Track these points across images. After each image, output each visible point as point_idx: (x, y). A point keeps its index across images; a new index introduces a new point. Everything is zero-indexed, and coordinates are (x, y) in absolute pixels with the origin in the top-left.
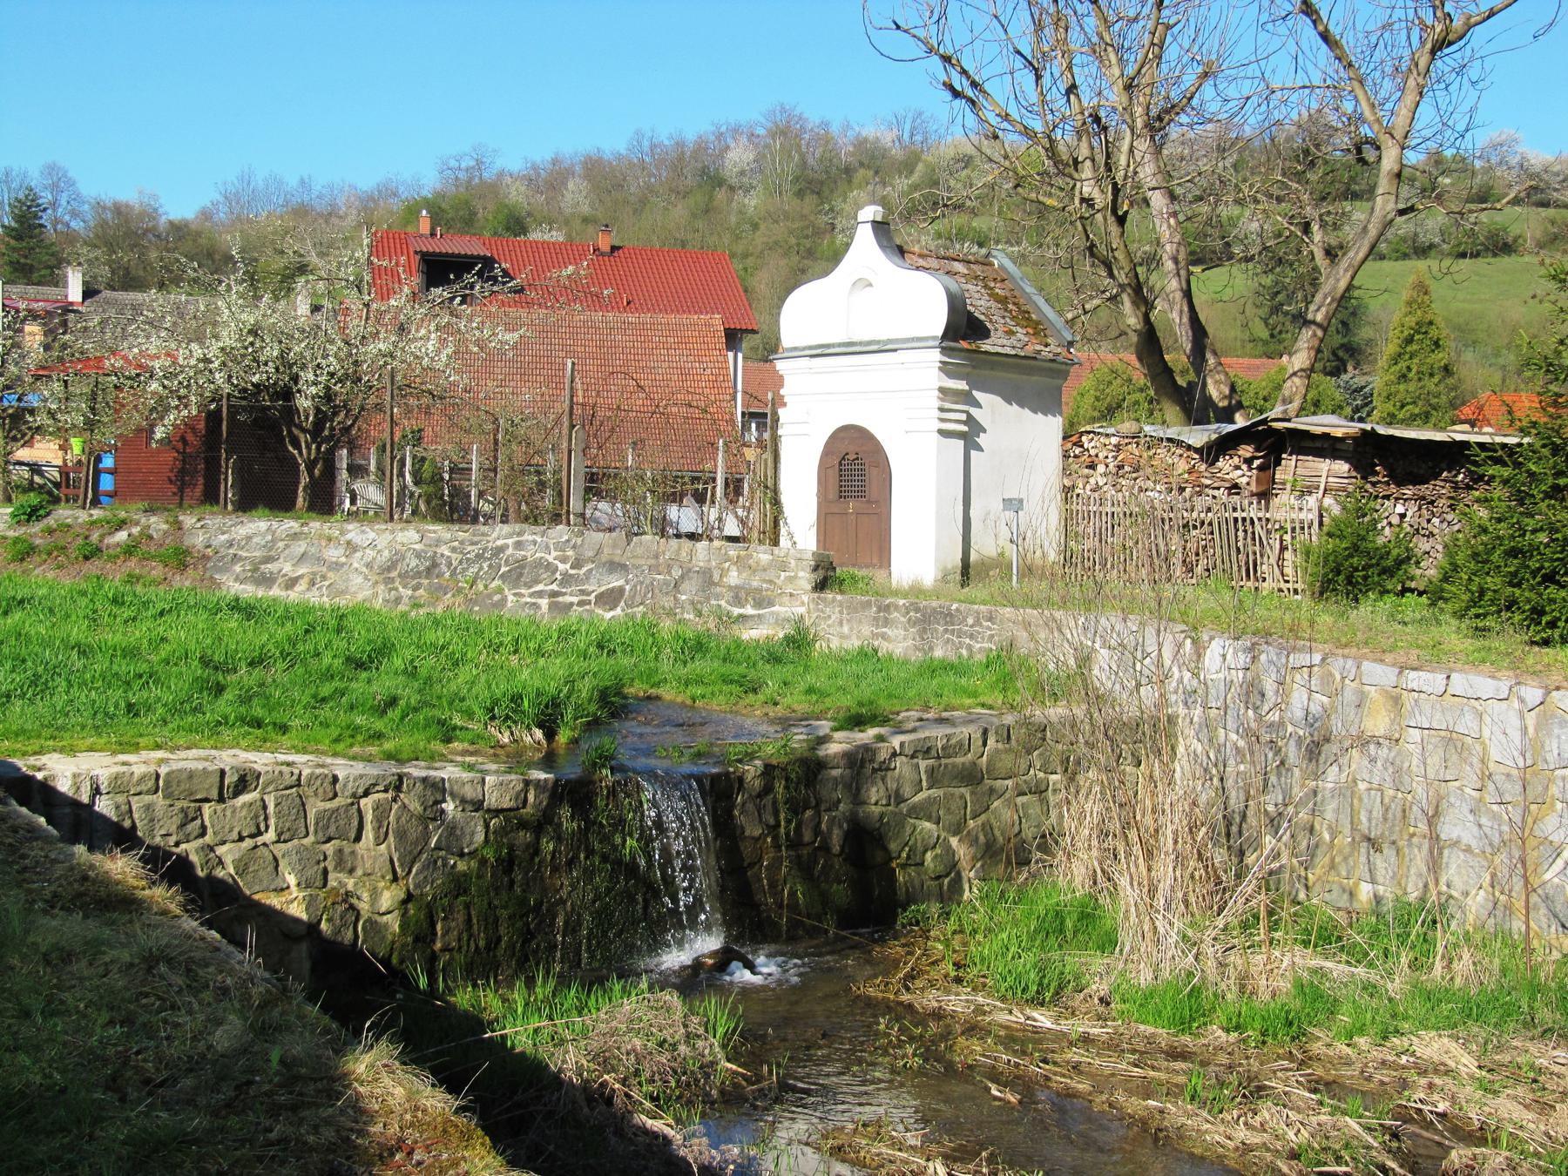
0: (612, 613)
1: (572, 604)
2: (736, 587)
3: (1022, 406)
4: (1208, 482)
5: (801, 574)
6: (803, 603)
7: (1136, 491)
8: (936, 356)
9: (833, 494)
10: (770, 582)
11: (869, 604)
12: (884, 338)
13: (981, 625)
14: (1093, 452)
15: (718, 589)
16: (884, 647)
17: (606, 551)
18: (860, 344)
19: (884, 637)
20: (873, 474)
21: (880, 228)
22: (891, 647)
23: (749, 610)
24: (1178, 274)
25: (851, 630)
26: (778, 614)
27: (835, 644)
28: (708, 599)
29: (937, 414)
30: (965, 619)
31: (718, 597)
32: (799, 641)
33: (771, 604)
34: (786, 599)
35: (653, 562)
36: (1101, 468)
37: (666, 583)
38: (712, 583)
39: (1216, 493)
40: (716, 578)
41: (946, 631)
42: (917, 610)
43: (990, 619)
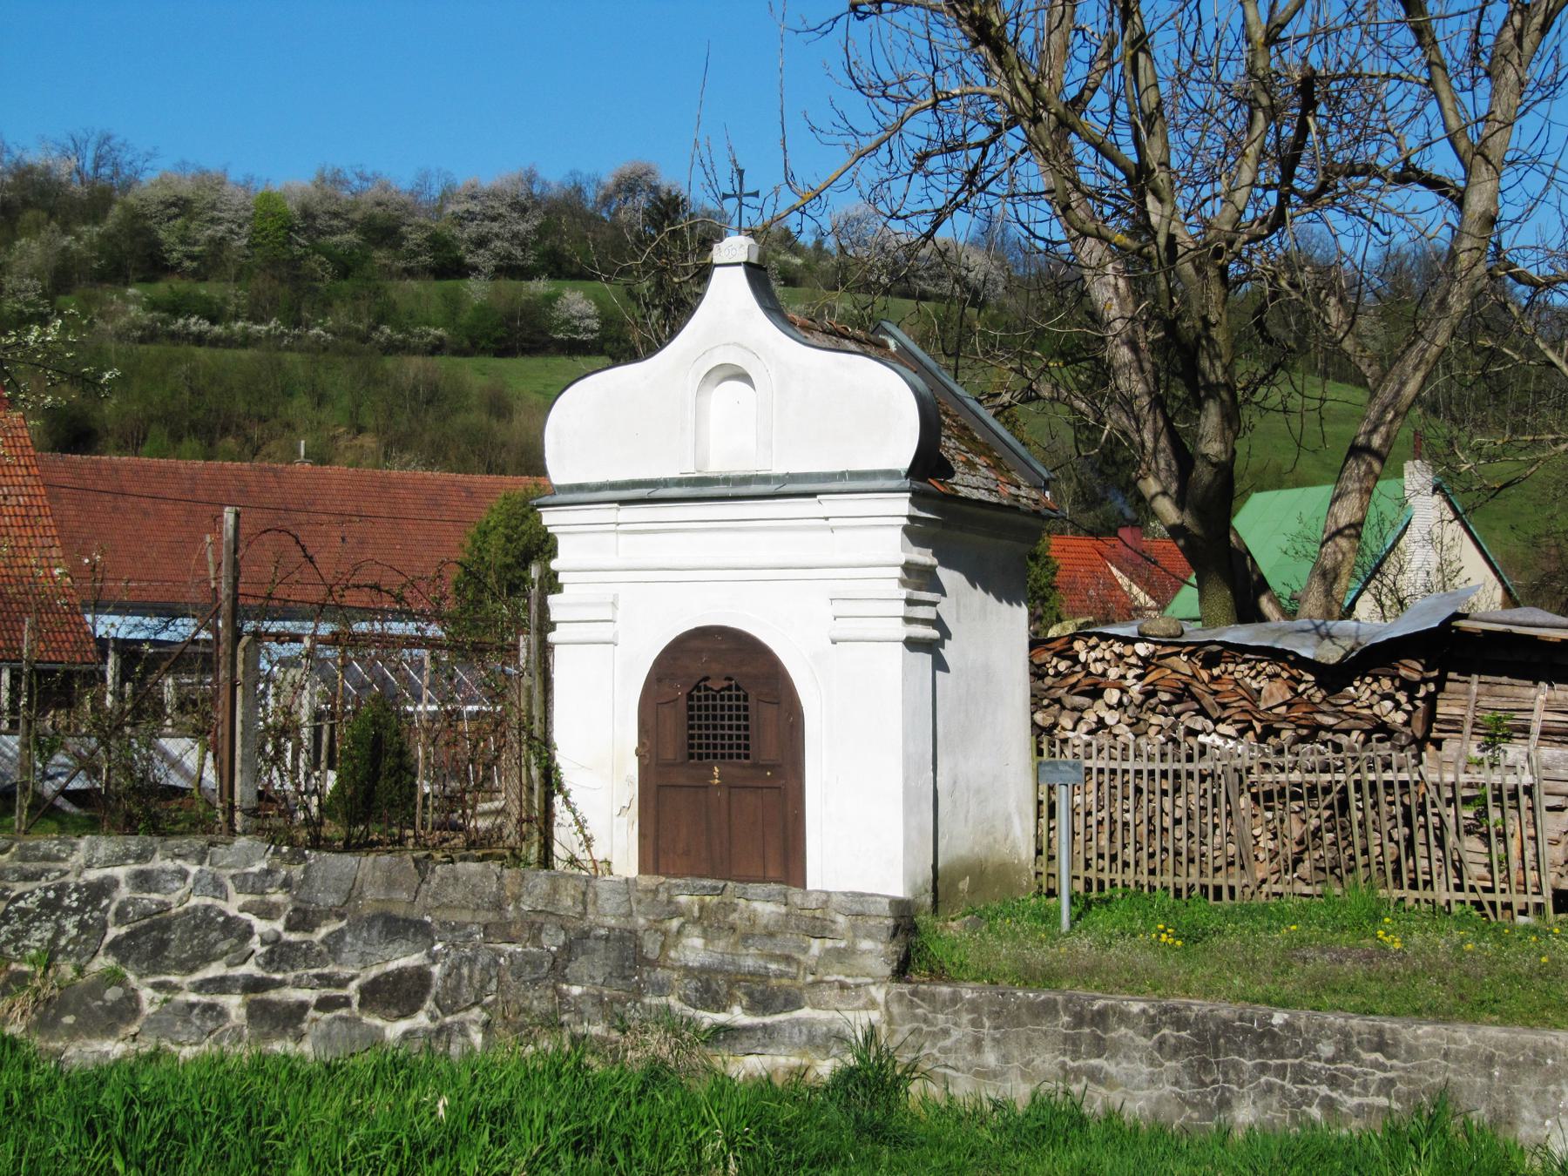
0: (403, 1025)
1: (303, 1006)
2: (703, 969)
3: (986, 590)
4: (1330, 721)
5: (866, 944)
6: (873, 1004)
7: (1180, 733)
8: (901, 505)
9: (672, 749)
10: (788, 959)
11: (1049, 1009)
12: (778, 469)
13: (1357, 1060)
14: (1097, 668)
15: (660, 974)
16: (1097, 1100)
17: (370, 894)
18: (726, 480)
19: (1095, 1076)
20: (764, 716)
21: (756, 273)
22: (1116, 1097)
23: (737, 1016)
24: (1142, 370)
25: (1006, 1059)
26: (810, 1024)
27: (963, 1088)
28: (639, 993)
29: (901, 609)
30: (1310, 1046)
31: (661, 989)
32: (872, 1082)
33: (792, 1002)
34: (830, 995)
35: (491, 916)
36: (1112, 696)
37: (533, 962)
38: (641, 960)
39: (1343, 739)
40: (651, 947)
41: (1263, 1069)
42: (1180, 1023)
43: (1381, 1046)
